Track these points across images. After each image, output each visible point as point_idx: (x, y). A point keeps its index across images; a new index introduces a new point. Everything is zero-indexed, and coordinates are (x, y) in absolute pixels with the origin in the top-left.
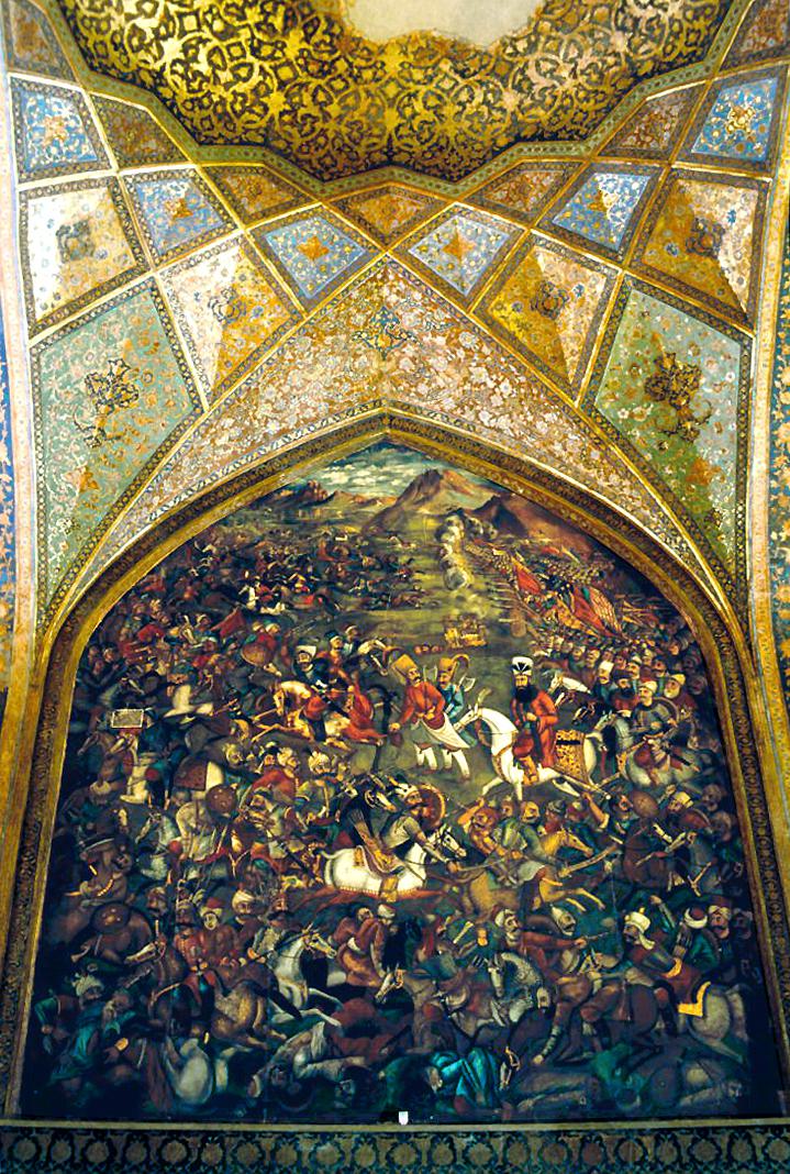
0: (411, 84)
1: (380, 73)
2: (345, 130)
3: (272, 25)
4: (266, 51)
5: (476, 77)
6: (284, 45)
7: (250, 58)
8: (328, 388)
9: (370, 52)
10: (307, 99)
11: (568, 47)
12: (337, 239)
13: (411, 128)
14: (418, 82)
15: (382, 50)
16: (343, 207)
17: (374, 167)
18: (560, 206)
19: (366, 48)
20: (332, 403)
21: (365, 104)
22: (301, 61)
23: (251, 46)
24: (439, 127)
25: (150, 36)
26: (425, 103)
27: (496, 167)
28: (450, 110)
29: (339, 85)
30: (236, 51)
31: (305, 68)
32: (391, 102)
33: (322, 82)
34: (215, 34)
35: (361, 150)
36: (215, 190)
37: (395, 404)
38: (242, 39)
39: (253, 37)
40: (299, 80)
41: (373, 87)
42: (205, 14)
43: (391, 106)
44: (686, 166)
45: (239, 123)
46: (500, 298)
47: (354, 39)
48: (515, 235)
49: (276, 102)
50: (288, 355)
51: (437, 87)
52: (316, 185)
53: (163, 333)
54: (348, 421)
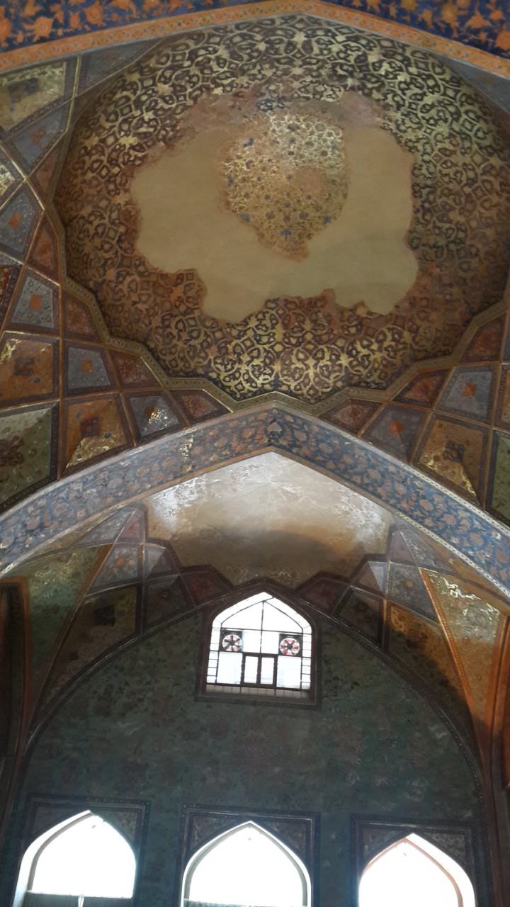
0: (108, 213)
1: (113, 193)
2: (78, 188)
3: (142, 126)
4: (125, 127)
5: (119, 250)
6: (128, 136)
7: (120, 119)
9: (124, 184)
10: (94, 158)
11: (147, 294)
12: (25, 230)
13: (84, 225)
14: (110, 217)
15: (127, 191)
16: (45, 222)
19: (127, 182)
21: (92, 191)
22: (118, 147)
23: (129, 118)
24: (86, 241)
26: (98, 226)
27: (81, 293)
28: (97, 241)
29: (104, 172)
31: (114, 150)
33: (105, 162)
34: (139, 97)
38: (134, 112)
39: (134, 118)
40: (106, 149)
42: (153, 90)
43: (94, 207)
44: (123, 400)
46: (18, 341)
47: (132, 173)
51: (109, 229)
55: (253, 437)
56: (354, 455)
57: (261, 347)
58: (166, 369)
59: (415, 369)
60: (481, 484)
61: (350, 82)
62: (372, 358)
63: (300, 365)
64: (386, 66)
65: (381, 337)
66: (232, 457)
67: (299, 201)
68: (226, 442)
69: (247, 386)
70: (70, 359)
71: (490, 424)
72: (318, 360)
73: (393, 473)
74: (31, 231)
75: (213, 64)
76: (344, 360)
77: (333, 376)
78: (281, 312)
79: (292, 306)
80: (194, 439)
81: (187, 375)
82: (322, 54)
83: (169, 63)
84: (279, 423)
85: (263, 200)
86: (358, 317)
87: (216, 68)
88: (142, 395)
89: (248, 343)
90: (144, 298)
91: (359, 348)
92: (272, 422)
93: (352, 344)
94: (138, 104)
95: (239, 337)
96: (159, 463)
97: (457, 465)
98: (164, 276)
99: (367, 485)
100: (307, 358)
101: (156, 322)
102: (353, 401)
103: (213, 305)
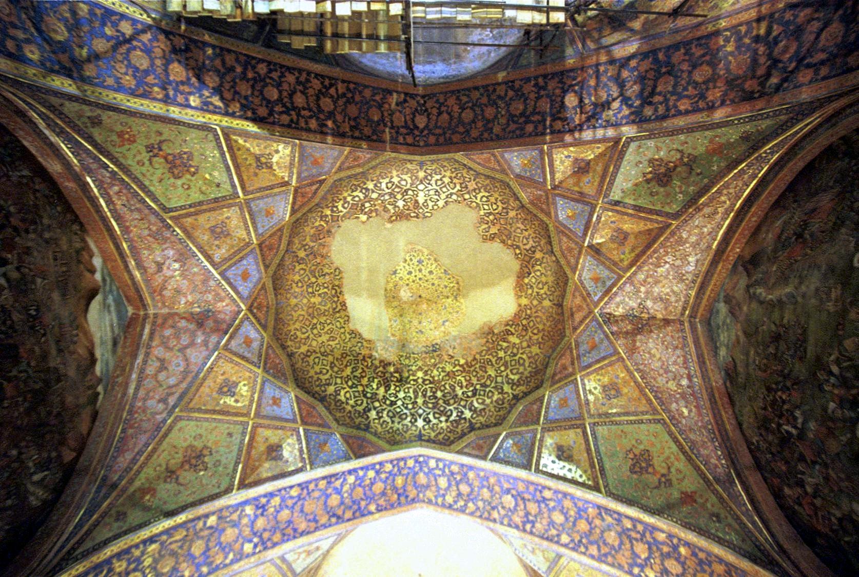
2: (548, 324)
4: (515, 351)
7: (517, 358)
8: (667, 348)
10: (536, 337)
16: (575, 329)
17: (563, 313)
18: (575, 233)
20: (677, 347)
21: (540, 314)
25: (500, 396)
27: (563, 262)
28: (544, 279)
29: (531, 324)
30: (513, 363)
32: (540, 303)
35: (557, 317)
36: (558, 385)
37: (682, 314)
41: (534, 310)
45: (540, 367)
48: (587, 253)
49: (535, 350)
50: (641, 367)
52: (566, 339)
53: (617, 427)
54: (690, 340)
55: (440, 113)
56: (350, 119)
57: (435, 187)
58: (508, 185)
59: (317, 200)
60: (230, 148)
61: (392, 369)
62: (349, 192)
63: (404, 177)
64: (375, 386)
65: (346, 205)
66: (459, 91)
67: (414, 281)
68: (463, 115)
69: (445, 164)
70: (582, 227)
71: (245, 200)
72: (390, 182)
73: (311, 117)
74: (584, 330)
75: (464, 384)
76: (370, 185)
77: (378, 173)
78: (421, 211)
79: (412, 215)
80: (492, 129)
81: (493, 178)
82: (408, 388)
83: (487, 390)
84: (417, 128)
85: (436, 282)
86: (365, 214)
87: (463, 379)
88: (530, 179)
89: (444, 189)
90: (519, 231)
91: (362, 196)
92: (424, 128)
93: (366, 196)
94: (506, 365)
95: (451, 194)
96: (526, 108)
97: (258, 152)
98: (503, 242)
99: (331, 85)
100: (399, 182)
101: (512, 214)
102: (359, 166)
103: (471, 216)
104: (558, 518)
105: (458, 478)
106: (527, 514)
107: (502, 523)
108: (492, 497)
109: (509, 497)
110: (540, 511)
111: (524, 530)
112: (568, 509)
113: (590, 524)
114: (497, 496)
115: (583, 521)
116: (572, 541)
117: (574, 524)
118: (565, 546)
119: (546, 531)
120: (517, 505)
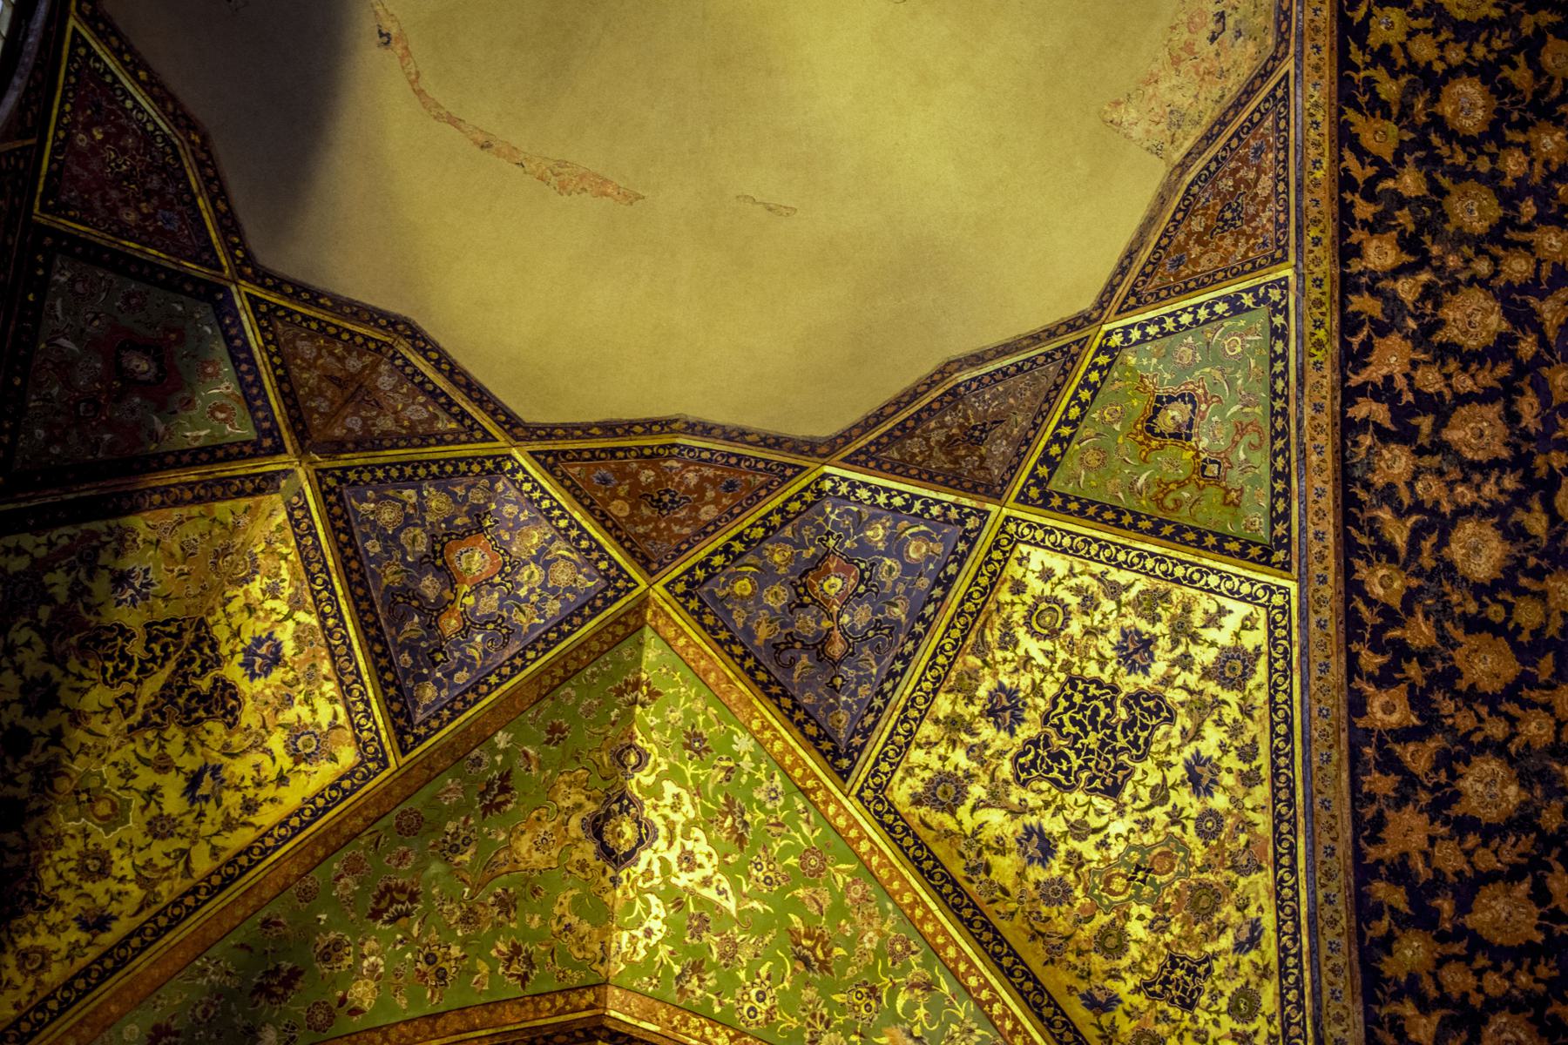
104: (1479, 552)
105: (1521, 76)
106: (1441, 408)
107: (1347, 285)
108: (1462, 238)
109: (1496, 322)
110: (1476, 466)
111: (1349, 396)
112: (1542, 596)
113: (1511, 692)
114: (1483, 267)
115: (1510, 669)
116: (1390, 616)
117: (1474, 625)
118: (1353, 587)
119: (1388, 494)
120: (1468, 359)
